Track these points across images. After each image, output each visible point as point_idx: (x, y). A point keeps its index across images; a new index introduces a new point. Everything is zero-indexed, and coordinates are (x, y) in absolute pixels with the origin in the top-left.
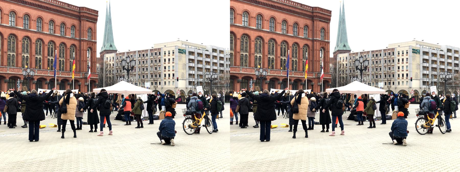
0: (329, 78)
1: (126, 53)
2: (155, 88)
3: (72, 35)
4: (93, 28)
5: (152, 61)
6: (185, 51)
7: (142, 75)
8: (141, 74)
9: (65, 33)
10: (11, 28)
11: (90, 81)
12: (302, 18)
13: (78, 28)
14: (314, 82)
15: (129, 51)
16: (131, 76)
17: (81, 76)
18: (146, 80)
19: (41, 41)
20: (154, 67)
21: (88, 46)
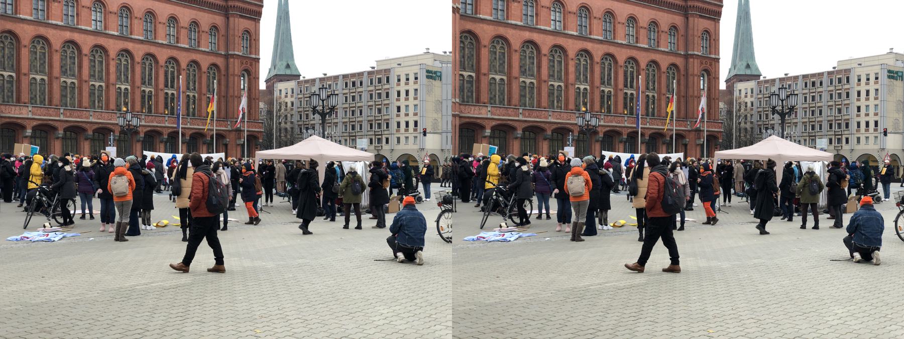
0: (719, 130)
1: (318, 81)
2: (378, 150)
3: (211, 45)
4: (252, 31)
5: (371, 95)
6: (441, 75)
7: (351, 123)
8: (374, 121)
9: (199, 42)
10: (95, 33)
11: (247, 136)
12: (664, 12)
13: (222, 31)
14: (689, 139)
15: (325, 76)
16: (329, 126)
17: (229, 126)
18: (359, 134)
19: (152, 59)
20: (375, 108)
21: (243, 66)
